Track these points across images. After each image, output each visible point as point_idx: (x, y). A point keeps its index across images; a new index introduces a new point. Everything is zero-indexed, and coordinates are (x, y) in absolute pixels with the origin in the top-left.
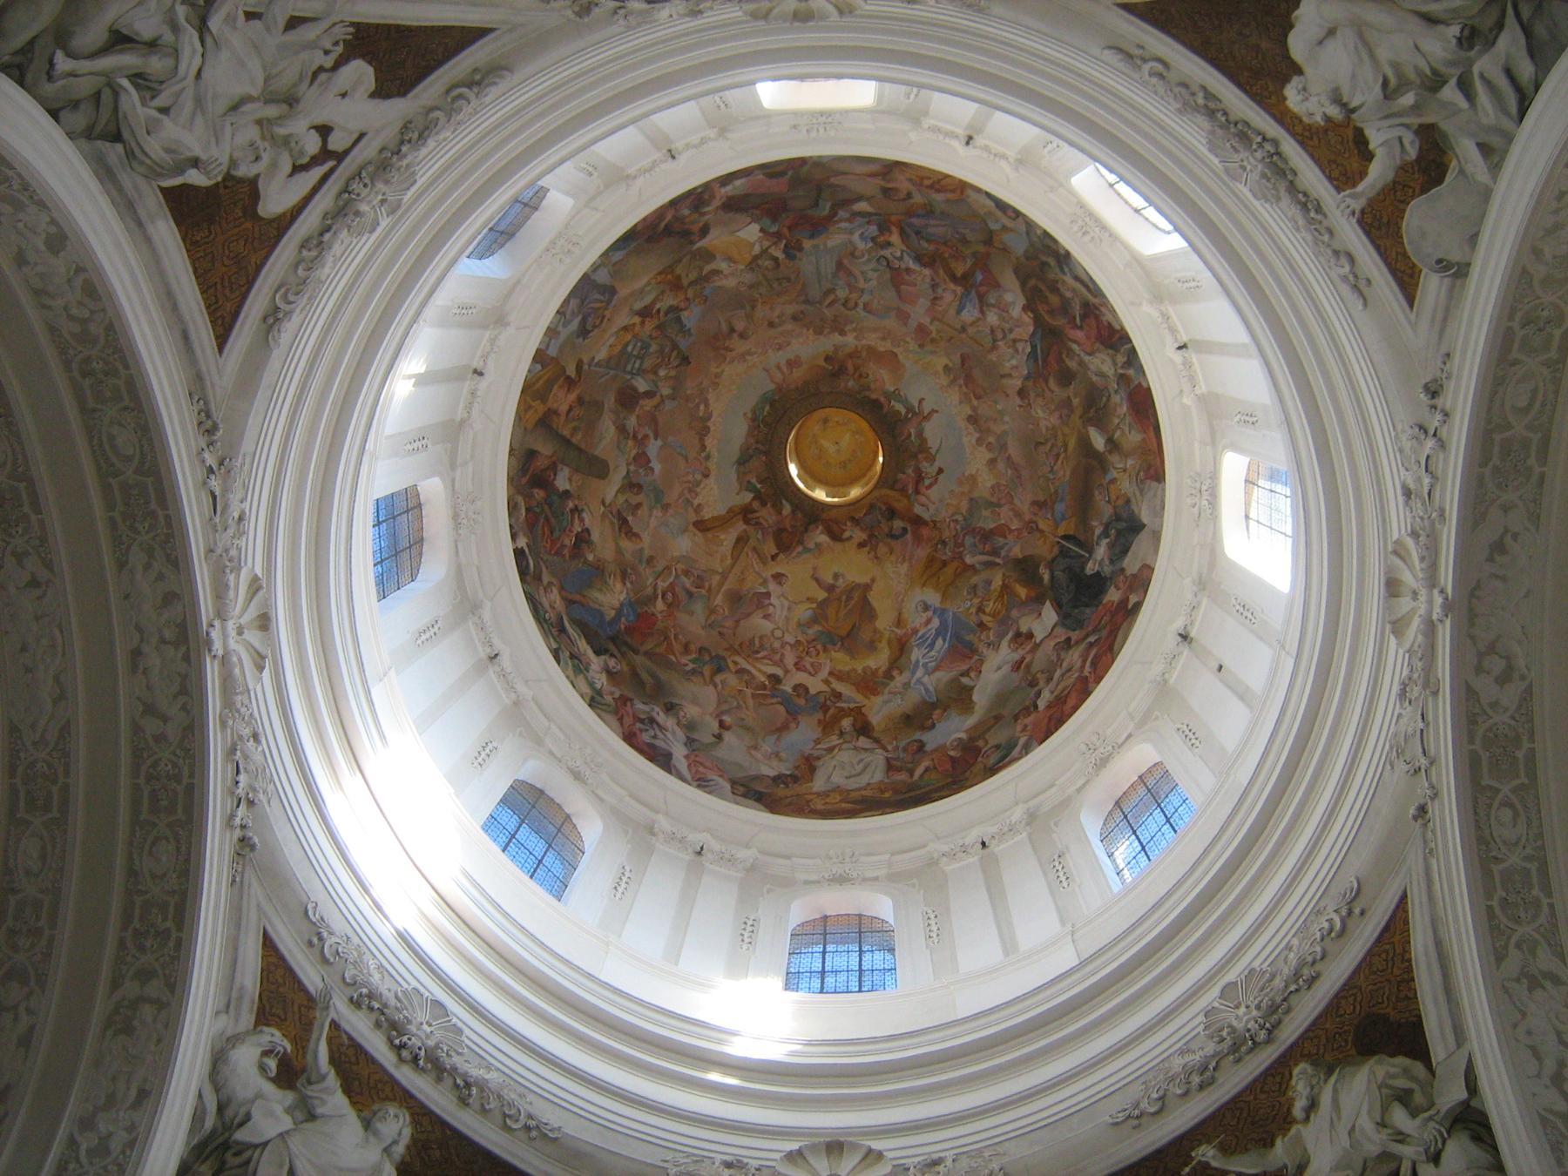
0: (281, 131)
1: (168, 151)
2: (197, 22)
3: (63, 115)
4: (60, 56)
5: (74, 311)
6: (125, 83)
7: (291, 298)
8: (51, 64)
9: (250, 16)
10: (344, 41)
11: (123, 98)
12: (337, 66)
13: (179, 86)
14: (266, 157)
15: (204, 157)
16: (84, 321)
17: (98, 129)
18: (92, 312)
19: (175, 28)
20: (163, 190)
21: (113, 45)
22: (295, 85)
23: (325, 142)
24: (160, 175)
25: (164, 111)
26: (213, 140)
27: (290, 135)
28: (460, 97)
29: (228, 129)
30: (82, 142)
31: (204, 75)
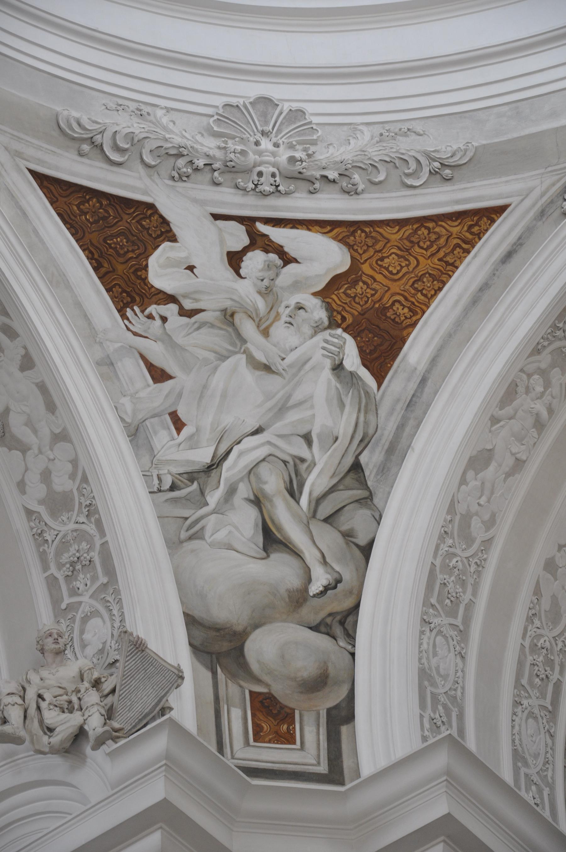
0: (261, 304)
1: (342, 405)
2: (214, 473)
3: (362, 541)
4: (315, 588)
5: (539, 389)
6: (304, 500)
7: (413, 166)
8: (326, 589)
9: (179, 425)
10: (143, 311)
11: (319, 491)
12: (171, 299)
13: (280, 443)
14: (293, 301)
15: (328, 364)
16: (543, 373)
17: (360, 493)
18: (529, 376)
19: (232, 491)
20: (380, 378)
21: (280, 542)
22: (212, 326)
23: (245, 250)
24: (367, 393)
25: (307, 438)
26: (307, 367)
27: (259, 293)
28: (117, 149)
29: (290, 359)
30: (376, 501)
31: (253, 425)
